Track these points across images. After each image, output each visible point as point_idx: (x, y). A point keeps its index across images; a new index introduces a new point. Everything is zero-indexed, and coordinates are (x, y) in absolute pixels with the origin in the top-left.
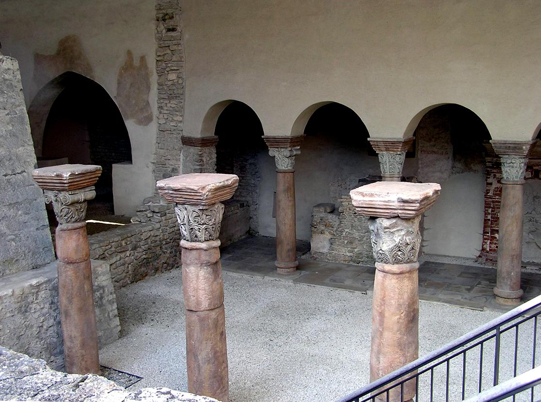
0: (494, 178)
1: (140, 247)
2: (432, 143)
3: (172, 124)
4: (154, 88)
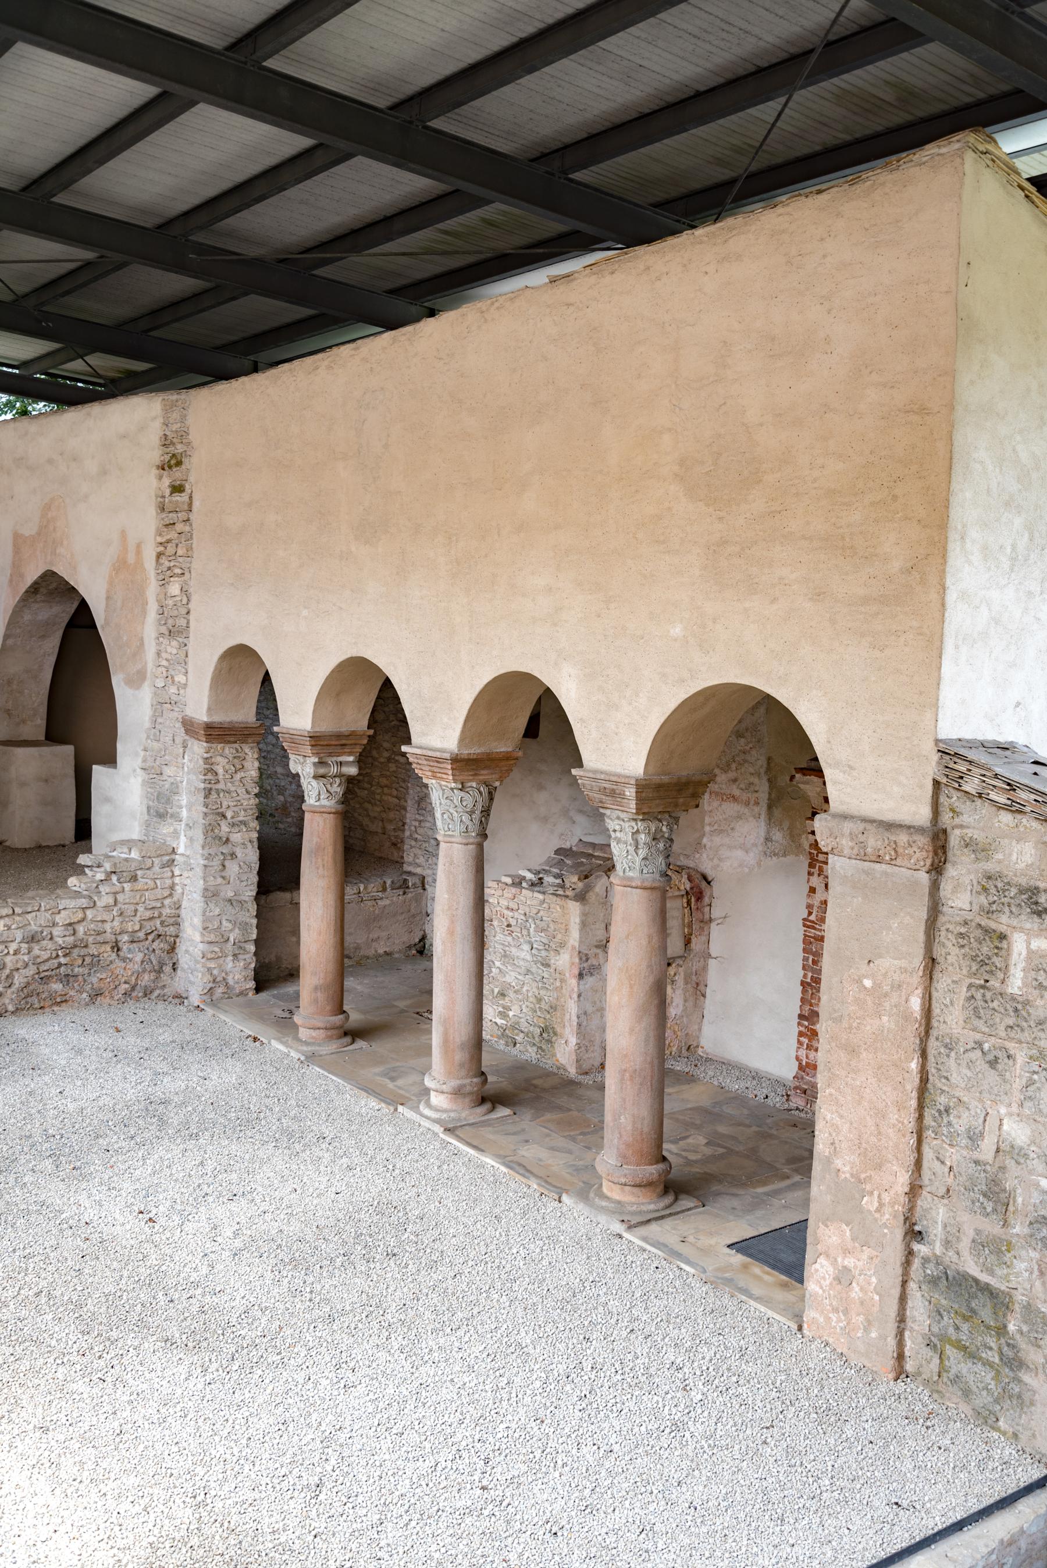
0: (819, 875)
1: (51, 939)
2: (732, 775)
3: (173, 690)
4: (153, 608)
